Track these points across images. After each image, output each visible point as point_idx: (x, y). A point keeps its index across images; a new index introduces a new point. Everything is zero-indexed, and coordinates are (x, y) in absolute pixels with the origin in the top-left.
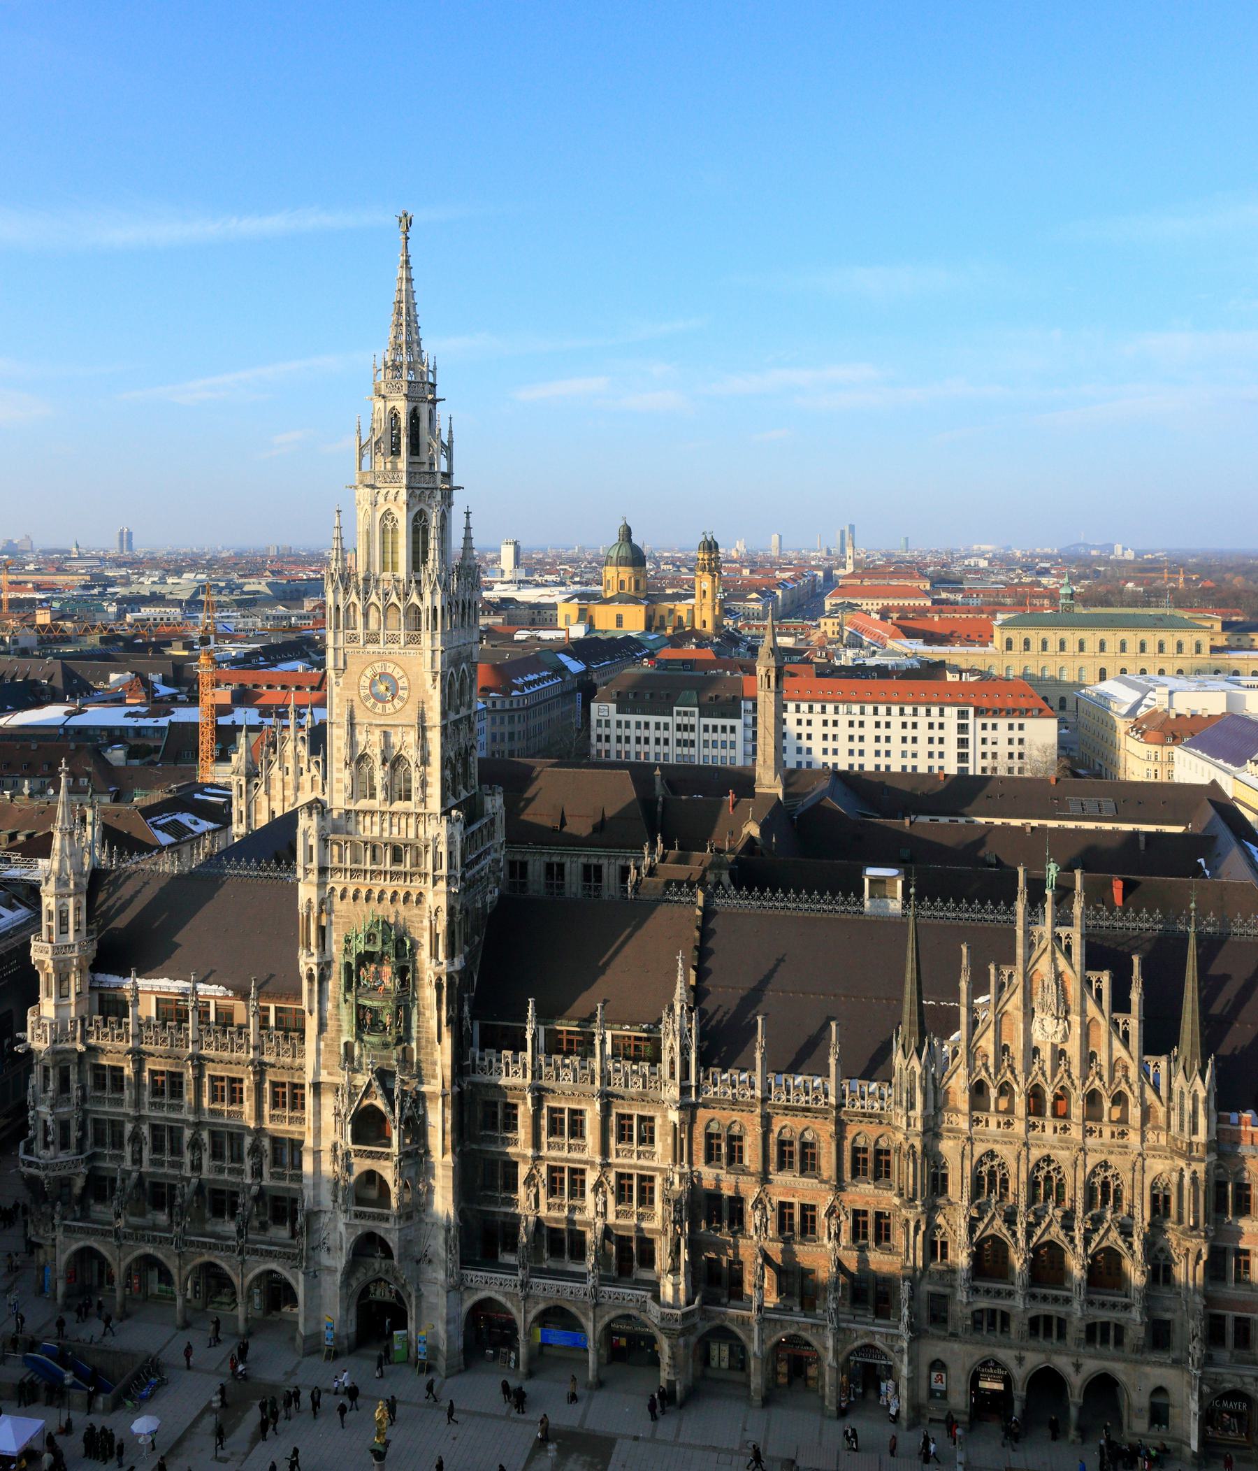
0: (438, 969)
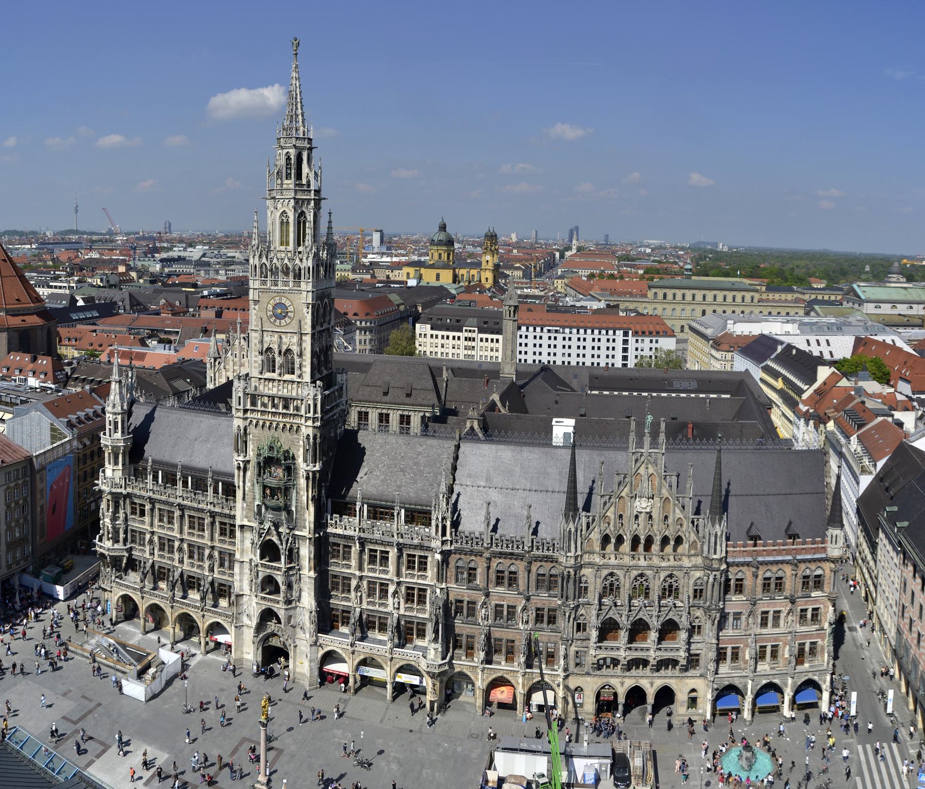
0: (308, 468)
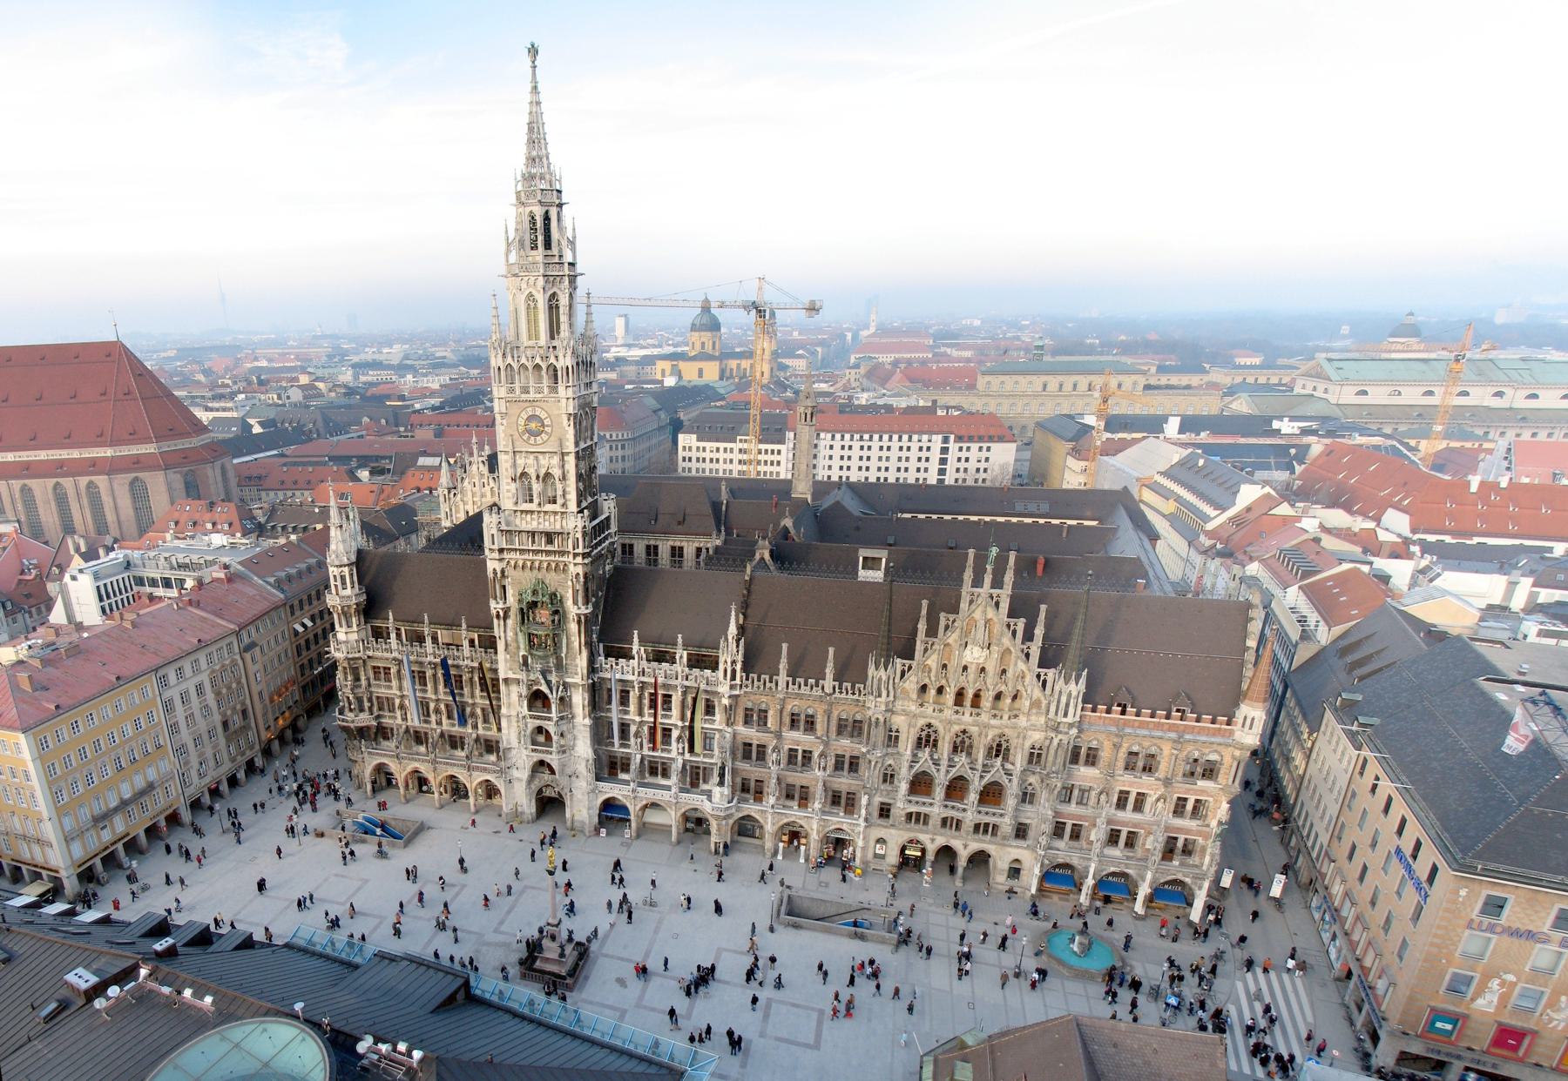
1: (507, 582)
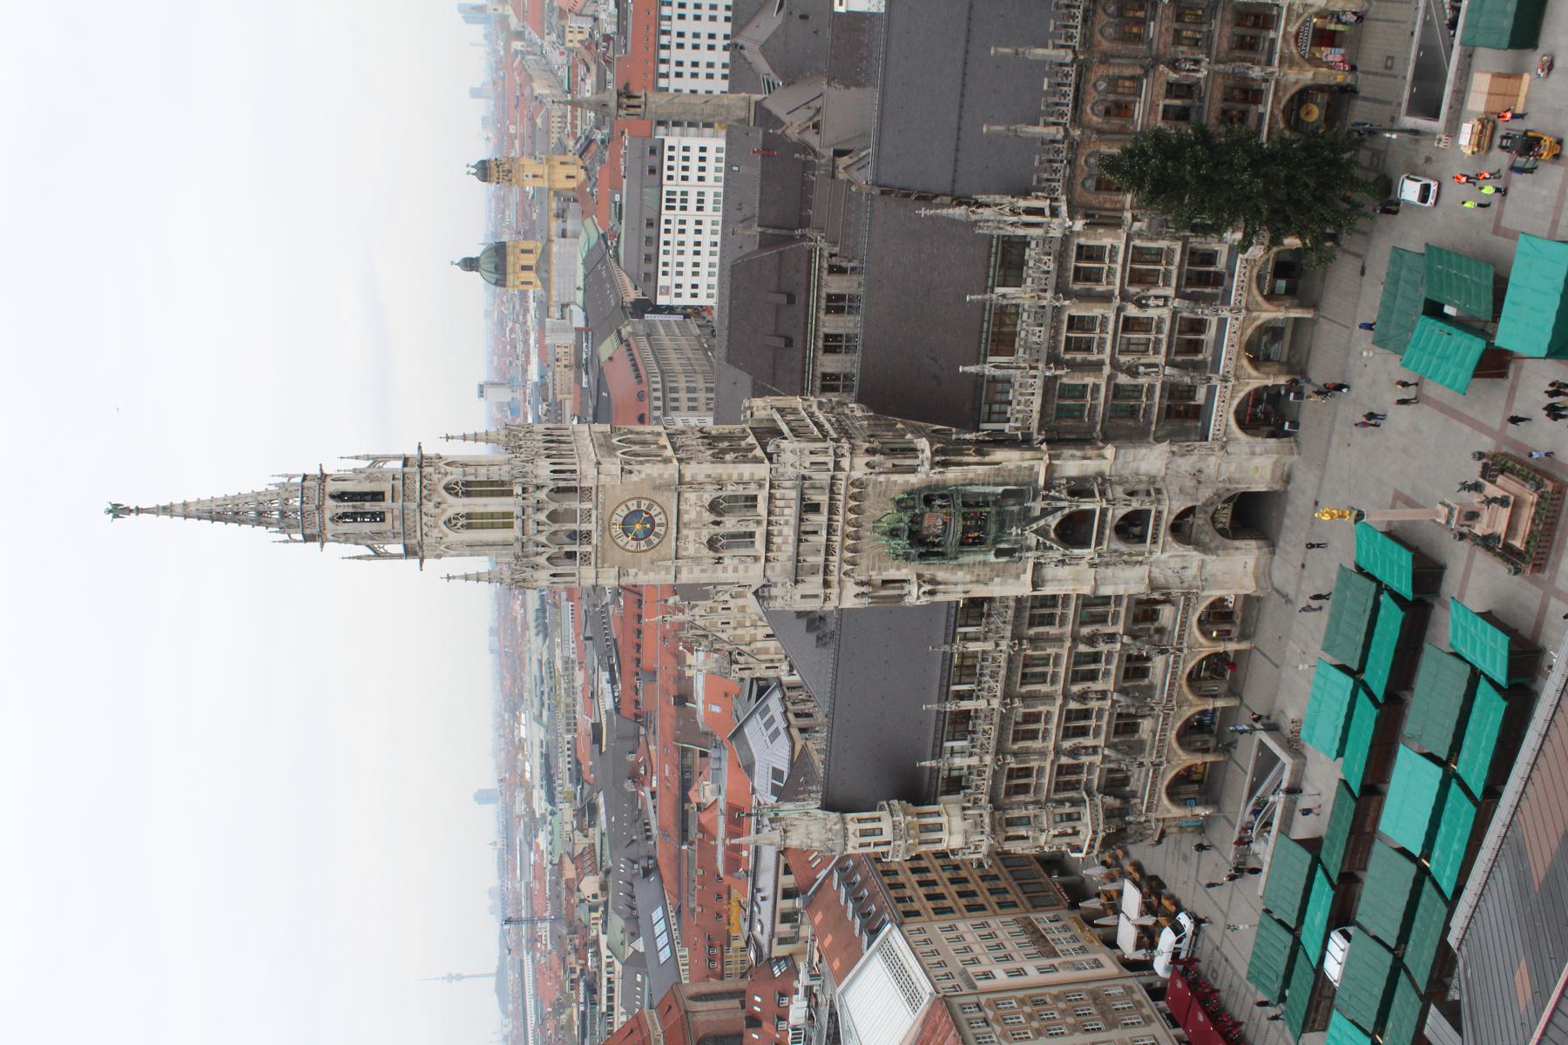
0: (927, 466)
1: (877, 577)
